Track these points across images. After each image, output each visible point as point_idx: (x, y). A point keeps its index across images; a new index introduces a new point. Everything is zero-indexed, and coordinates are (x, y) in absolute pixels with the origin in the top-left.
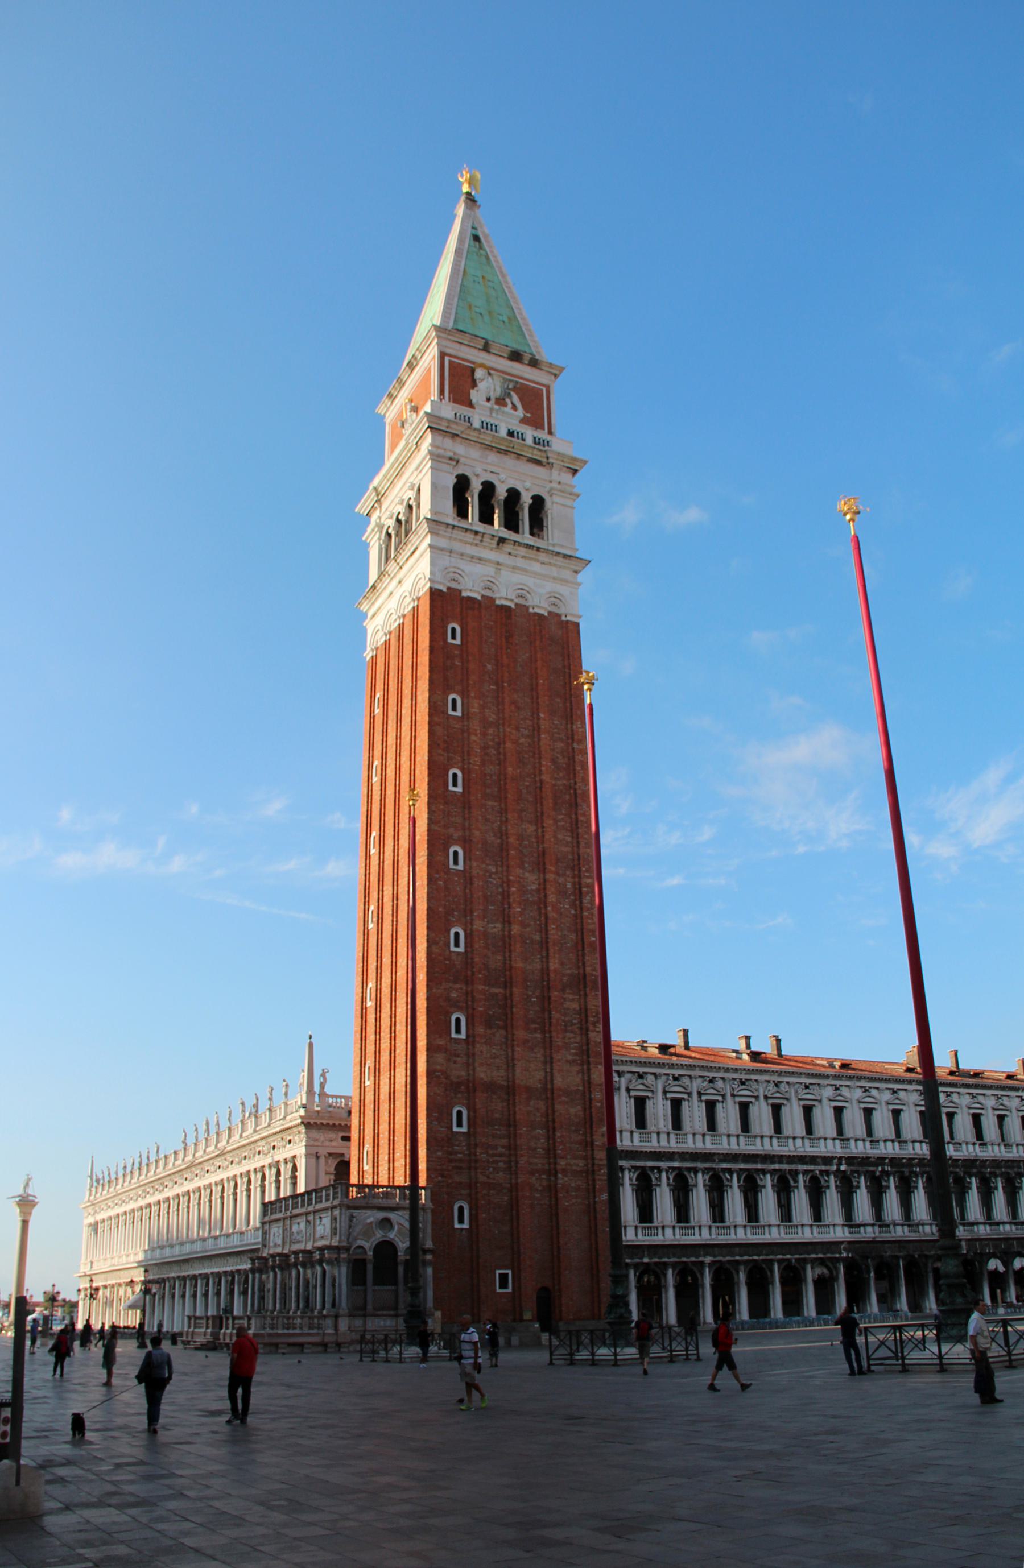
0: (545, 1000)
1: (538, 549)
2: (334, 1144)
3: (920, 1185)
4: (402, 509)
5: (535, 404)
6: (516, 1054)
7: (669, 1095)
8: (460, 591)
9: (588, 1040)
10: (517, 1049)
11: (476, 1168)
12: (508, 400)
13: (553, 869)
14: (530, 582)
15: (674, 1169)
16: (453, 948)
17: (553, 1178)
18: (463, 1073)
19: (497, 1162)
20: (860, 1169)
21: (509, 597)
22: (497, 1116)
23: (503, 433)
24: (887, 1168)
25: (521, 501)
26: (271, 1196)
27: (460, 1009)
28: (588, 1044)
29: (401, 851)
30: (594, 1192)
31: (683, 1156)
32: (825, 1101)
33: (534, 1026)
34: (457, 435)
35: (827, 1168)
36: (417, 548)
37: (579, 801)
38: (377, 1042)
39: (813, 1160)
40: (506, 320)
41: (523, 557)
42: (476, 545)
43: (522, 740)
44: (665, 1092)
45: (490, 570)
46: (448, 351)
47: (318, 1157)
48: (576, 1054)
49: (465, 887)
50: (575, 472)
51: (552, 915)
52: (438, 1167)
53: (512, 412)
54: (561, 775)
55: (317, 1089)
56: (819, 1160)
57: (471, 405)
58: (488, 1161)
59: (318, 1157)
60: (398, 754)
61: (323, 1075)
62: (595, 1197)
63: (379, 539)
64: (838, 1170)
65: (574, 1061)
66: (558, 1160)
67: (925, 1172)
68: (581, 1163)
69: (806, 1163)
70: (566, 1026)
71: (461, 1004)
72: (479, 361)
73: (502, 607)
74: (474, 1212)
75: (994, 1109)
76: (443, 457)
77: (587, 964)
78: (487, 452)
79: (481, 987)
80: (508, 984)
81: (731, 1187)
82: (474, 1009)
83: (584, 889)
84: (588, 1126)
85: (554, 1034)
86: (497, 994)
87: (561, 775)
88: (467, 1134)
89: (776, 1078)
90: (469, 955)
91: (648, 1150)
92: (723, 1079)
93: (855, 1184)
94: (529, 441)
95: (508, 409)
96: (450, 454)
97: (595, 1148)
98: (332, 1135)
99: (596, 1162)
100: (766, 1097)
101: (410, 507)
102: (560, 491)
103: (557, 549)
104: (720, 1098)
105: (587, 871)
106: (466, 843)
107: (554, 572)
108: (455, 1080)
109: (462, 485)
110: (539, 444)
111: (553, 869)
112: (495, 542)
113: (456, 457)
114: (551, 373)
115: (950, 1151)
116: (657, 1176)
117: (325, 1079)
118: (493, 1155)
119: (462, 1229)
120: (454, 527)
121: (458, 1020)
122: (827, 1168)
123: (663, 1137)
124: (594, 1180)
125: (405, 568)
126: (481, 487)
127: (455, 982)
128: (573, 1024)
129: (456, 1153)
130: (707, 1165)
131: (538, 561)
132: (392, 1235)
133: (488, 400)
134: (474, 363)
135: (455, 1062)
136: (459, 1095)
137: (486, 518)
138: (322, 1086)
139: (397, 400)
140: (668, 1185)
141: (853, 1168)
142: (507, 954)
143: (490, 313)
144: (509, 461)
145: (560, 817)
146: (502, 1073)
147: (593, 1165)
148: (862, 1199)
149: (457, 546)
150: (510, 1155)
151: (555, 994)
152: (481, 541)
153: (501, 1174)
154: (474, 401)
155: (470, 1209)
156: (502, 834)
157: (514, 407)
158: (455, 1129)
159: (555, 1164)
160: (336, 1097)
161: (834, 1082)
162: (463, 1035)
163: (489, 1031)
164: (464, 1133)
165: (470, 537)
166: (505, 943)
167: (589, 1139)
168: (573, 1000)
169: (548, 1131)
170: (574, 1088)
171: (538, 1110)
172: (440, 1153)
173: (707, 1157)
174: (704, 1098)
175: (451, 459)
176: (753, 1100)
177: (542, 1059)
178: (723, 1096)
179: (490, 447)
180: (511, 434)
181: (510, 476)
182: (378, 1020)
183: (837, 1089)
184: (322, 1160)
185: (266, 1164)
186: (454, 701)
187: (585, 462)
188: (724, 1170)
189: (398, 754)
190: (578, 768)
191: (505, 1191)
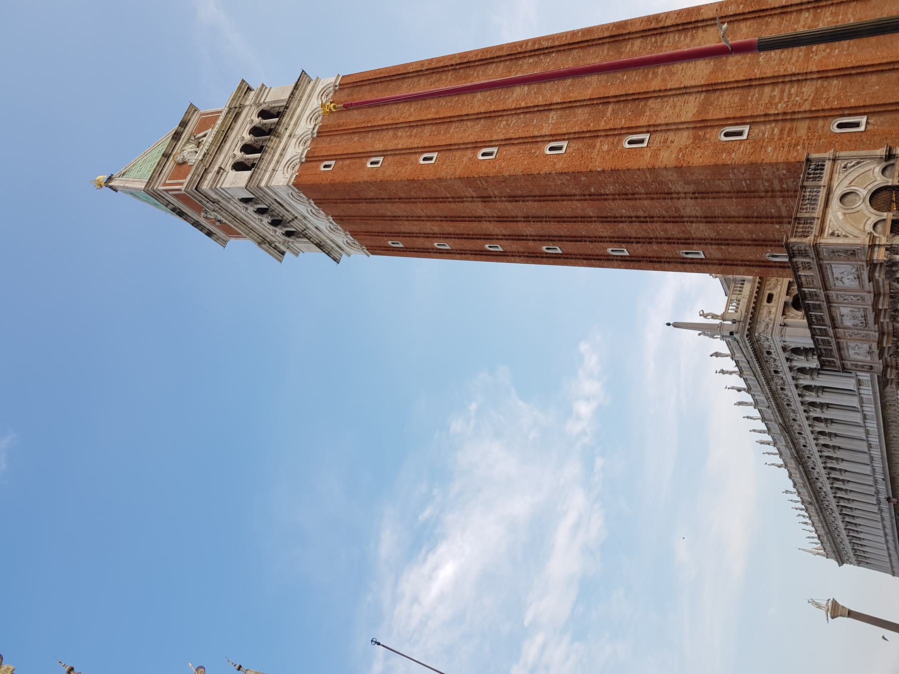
2: (773, 310)
6: (673, 87)
8: (302, 163)
9: (673, 26)
10: (669, 87)
11: (794, 113)
14: (307, 113)
18: (685, 133)
19: (790, 95)
21: (312, 127)
22: (737, 99)
25: (260, 126)
26: (814, 363)
28: (678, 25)
33: (650, 75)
37: (465, 61)
43: (412, 110)
46: (163, 181)
47: (785, 325)
49: (513, 144)
50: (249, 89)
52: (786, 149)
55: (717, 322)
59: (785, 325)
60: (419, 218)
61: (705, 316)
71: (616, 141)
76: (216, 178)
82: (622, 128)
83: (536, 47)
86: (613, 110)
90: (572, 136)
98: (764, 312)
105: (521, 47)
106: (476, 145)
109: (239, 166)
117: (708, 315)
118: (781, 98)
119: (867, 123)
121: (630, 143)
128: (656, 42)
132: (864, 193)
135: (672, 142)
137: (260, 150)
138: (714, 317)
142: (578, 104)
146: (692, 98)
153: (804, 89)
155: (843, 116)
157: (205, 136)
162: (646, 137)
163: (648, 113)
166: (569, 106)
171: (737, 62)
172: (769, 149)
181: (242, 133)
184: (789, 321)
185: (793, 382)
187: (243, 81)
190: (441, 64)
191: (826, 83)
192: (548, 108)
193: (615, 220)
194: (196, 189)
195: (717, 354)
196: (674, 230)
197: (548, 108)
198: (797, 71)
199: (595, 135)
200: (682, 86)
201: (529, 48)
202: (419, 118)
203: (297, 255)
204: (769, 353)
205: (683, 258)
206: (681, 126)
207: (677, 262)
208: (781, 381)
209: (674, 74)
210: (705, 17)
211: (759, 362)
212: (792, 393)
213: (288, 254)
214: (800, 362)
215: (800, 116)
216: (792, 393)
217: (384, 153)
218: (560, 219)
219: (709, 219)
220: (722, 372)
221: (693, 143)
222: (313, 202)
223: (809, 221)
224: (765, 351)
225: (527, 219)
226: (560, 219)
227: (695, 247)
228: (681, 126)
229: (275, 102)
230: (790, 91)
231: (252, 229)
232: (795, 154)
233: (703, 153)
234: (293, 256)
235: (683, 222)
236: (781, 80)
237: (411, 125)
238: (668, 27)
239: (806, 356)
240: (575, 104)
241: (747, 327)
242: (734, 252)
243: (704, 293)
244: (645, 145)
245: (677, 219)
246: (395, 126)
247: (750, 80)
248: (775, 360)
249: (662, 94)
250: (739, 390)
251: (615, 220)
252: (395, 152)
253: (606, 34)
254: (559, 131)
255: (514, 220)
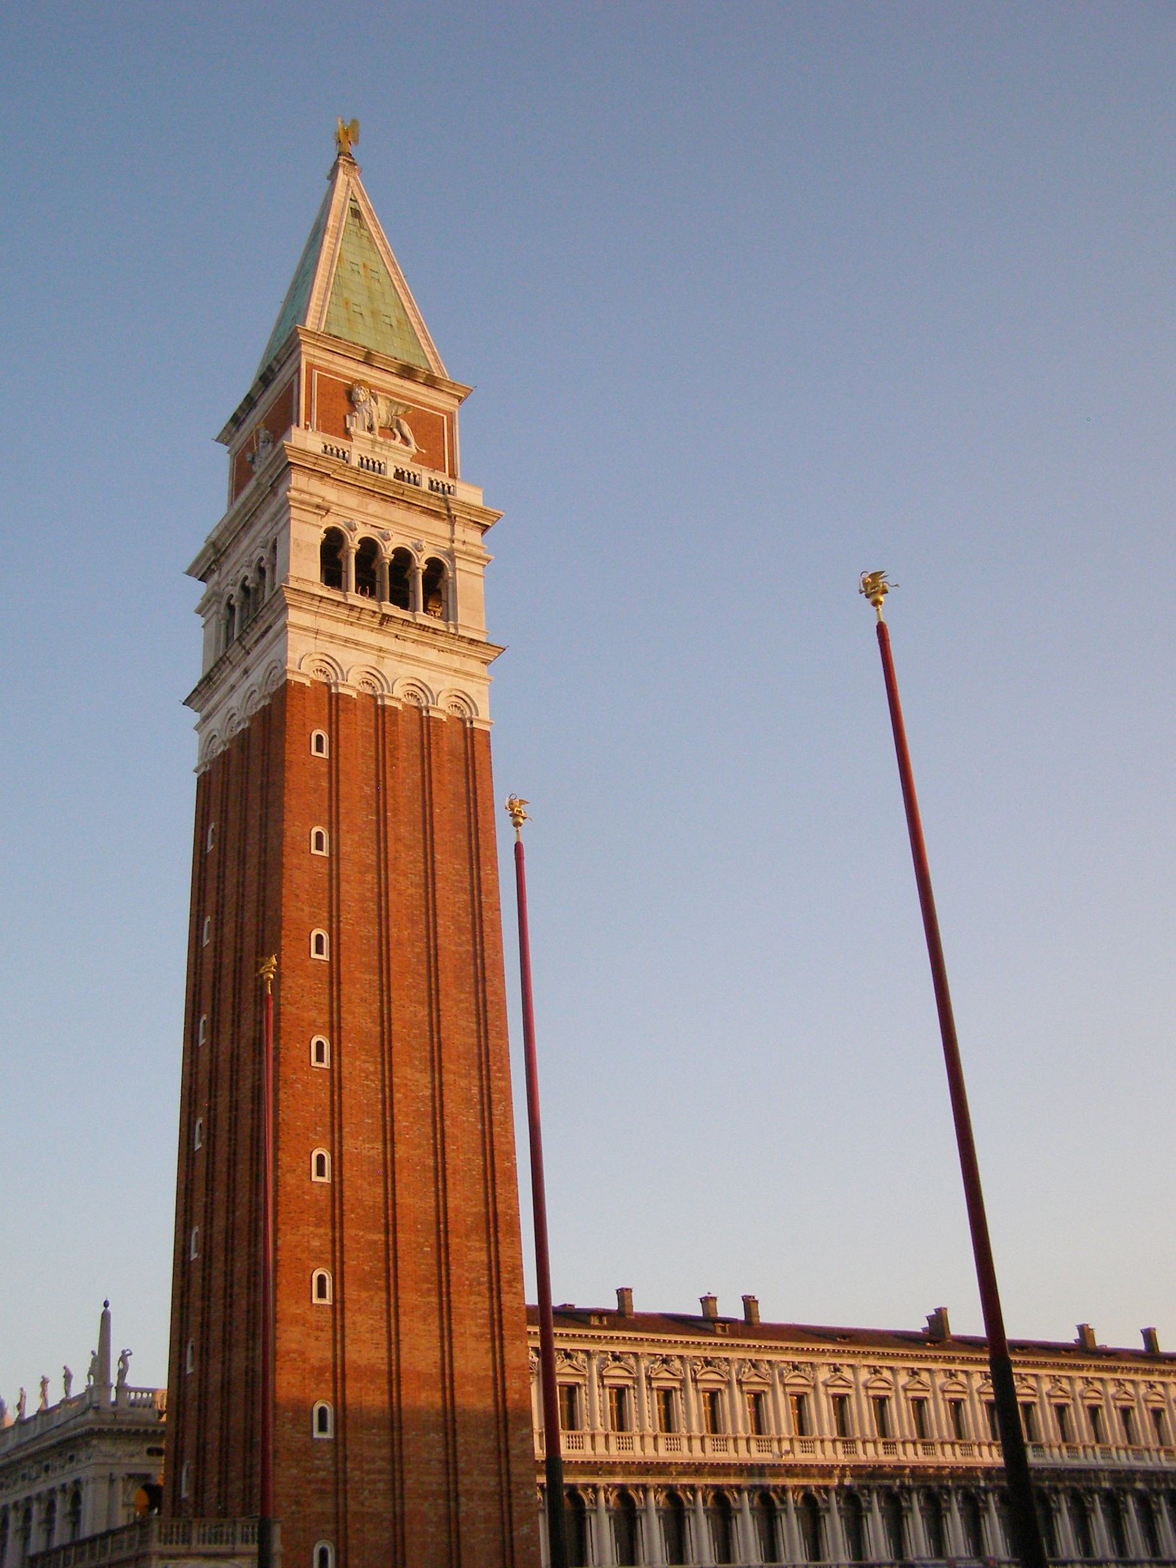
0: (442, 1249)
1: (435, 631)
2: (136, 1460)
3: (955, 1507)
4: (250, 573)
5: (431, 437)
7: (606, 1382)
8: (329, 686)
9: (500, 1305)
11: (345, 1492)
12: (395, 430)
13: (452, 1067)
14: (424, 675)
15: (616, 1486)
16: (315, 1178)
17: (452, 1504)
19: (375, 1482)
20: (871, 1483)
23: (390, 474)
24: (909, 1482)
27: (322, 1262)
28: (500, 1311)
29: (243, 1042)
30: (511, 1525)
31: (628, 1468)
32: (821, 1388)
33: (426, 1286)
34: (328, 475)
35: (827, 1482)
36: (270, 627)
37: (488, 973)
38: (205, 1311)
39: (805, 1470)
40: (394, 323)
41: (414, 641)
42: (352, 624)
44: (602, 1377)
45: (370, 659)
46: (317, 362)
47: (112, 1481)
48: (483, 1326)
50: (485, 528)
51: (449, 1130)
53: (402, 446)
54: (464, 938)
55: (114, 1379)
56: (814, 1471)
57: (347, 434)
58: (362, 1480)
59: (112, 1481)
60: (240, 908)
61: (123, 1358)
62: (511, 1532)
63: (217, 612)
64: (841, 1485)
65: (482, 1335)
66: (461, 1478)
67: (959, 1487)
68: (493, 1481)
69: (796, 1476)
70: (470, 1285)
72: (358, 376)
73: (384, 707)
74: (341, 1557)
75: (1115, 1399)
76: (309, 504)
77: (500, 1199)
78: (367, 500)
79: (353, 1232)
80: (390, 1228)
81: (695, 1511)
83: (495, 1096)
84: (501, 1426)
85: (454, 1297)
86: (375, 1242)
87: (464, 938)
88: (335, 1442)
89: (754, 1356)
91: (580, 1460)
92: (680, 1357)
93: (864, 1504)
94: (425, 486)
95: (397, 443)
96: (318, 501)
97: (512, 1459)
99: (513, 1479)
100: (740, 1382)
101: (261, 571)
102: (465, 553)
103: (461, 632)
104: (677, 1385)
105: (499, 1071)
106: (335, 1030)
107: (456, 662)
108: (316, 1364)
109: (333, 543)
110: (437, 489)
111: (452, 1067)
112: (377, 620)
113: (326, 504)
114: (455, 396)
115: (1032, 1458)
116: (592, 1496)
118: (369, 1472)
120: (322, 599)
122: (827, 1482)
123: (742, 1444)
124: (510, 1505)
125: (253, 654)
126: (358, 546)
127: (317, 1226)
128: (479, 1284)
129: (318, 1470)
130: (662, 1480)
131: (435, 647)
133: (370, 429)
134: (350, 379)
135: (317, 1339)
136: (322, 1386)
138: (122, 1374)
139: (244, 426)
140: (608, 1510)
141: (861, 1482)
143: (374, 313)
144: (397, 513)
145: (463, 996)
146: (383, 1353)
147: (509, 1482)
148: (876, 1525)
149: (326, 625)
150: (394, 1470)
151: (454, 1241)
152: (358, 619)
153: (380, 1500)
154: (352, 429)
155: (337, 1552)
156: (385, 1020)
158: (317, 1435)
159: (456, 1483)
160: (142, 1391)
161: (831, 1360)
162: (328, 1301)
163: (364, 1294)
164: (329, 1440)
165: (343, 613)
166: (388, 1170)
167: (502, 1446)
168: (481, 1249)
169: (446, 1435)
170: (482, 1373)
173: (660, 1468)
174: (655, 1384)
175: (318, 507)
176: (722, 1387)
177: (437, 1332)
178: (683, 1382)
179: (372, 493)
180: (399, 475)
182: (206, 1279)
183: (836, 1370)
184: (119, 1485)
186: (319, 836)
188: (684, 1487)
189: (240, 908)
191: (385, 1524)
192: (389, 1137)
193: (229, 1250)
194: (290, 463)
195: (68, 1377)
196: (216, 1333)
197: (389, 1137)
198: (406, 1486)
199: (337, 1222)
200: (401, 1337)
201: (495, 1084)
202: (392, 909)
203: (199, 611)
204: (72, 1458)
205: (187, 1342)
206: (339, 1346)
207: (181, 1333)
208: (34, 1475)
209: (425, 1320)
210: (506, 1350)
211: (59, 1444)
212: (18, 1493)
213: (201, 588)
214: (62, 1506)
215: (341, 1501)
216: (18, 1493)
217: (335, 857)
218: (232, 1163)
219: (226, 1387)
220: (44, 1383)
221: (313, 1367)
222: (267, 702)
223: (187, 1540)
224: (74, 1452)
225: (234, 1106)
226: (232, 1163)
227: (197, 1363)
228: (339, 1346)
229: (455, 591)
230: (380, 1481)
231: (237, 539)
232: (284, 1504)
233: (293, 1386)
234: (197, 602)
235: (224, 1351)
236: (396, 1466)
237: (382, 894)
238: (499, 1297)
239: (70, 1514)
240: (390, 1181)
241: (106, 1428)
242: (192, 1415)
243: (149, 1370)
244: (315, 1300)
245: (227, 1344)
246: (382, 865)
247: (401, 1428)
248: (63, 1467)
249: (393, 1311)
250: (19, 1406)
251: (229, 1250)
252: (334, 878)
253: (501, 1207)
254: (346, 1165)
255: (234, 1086)
